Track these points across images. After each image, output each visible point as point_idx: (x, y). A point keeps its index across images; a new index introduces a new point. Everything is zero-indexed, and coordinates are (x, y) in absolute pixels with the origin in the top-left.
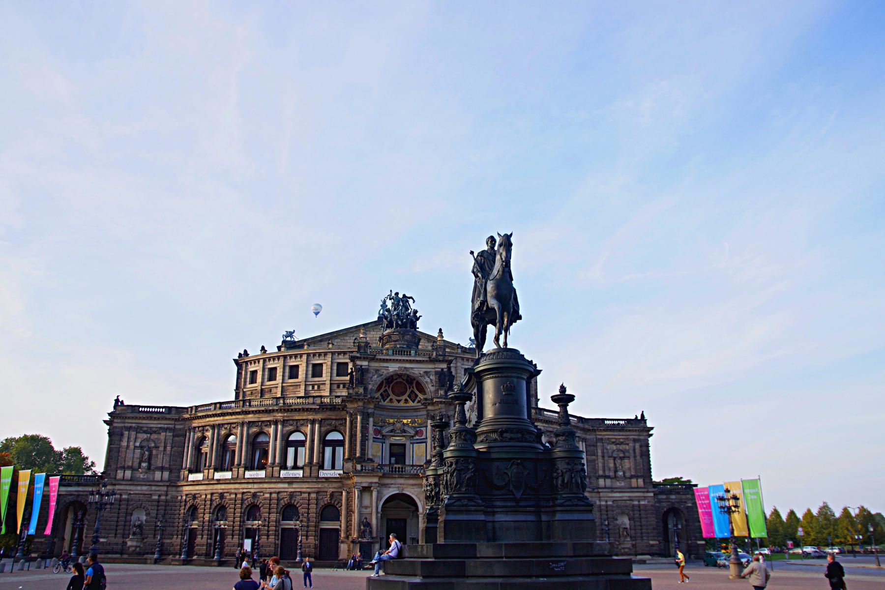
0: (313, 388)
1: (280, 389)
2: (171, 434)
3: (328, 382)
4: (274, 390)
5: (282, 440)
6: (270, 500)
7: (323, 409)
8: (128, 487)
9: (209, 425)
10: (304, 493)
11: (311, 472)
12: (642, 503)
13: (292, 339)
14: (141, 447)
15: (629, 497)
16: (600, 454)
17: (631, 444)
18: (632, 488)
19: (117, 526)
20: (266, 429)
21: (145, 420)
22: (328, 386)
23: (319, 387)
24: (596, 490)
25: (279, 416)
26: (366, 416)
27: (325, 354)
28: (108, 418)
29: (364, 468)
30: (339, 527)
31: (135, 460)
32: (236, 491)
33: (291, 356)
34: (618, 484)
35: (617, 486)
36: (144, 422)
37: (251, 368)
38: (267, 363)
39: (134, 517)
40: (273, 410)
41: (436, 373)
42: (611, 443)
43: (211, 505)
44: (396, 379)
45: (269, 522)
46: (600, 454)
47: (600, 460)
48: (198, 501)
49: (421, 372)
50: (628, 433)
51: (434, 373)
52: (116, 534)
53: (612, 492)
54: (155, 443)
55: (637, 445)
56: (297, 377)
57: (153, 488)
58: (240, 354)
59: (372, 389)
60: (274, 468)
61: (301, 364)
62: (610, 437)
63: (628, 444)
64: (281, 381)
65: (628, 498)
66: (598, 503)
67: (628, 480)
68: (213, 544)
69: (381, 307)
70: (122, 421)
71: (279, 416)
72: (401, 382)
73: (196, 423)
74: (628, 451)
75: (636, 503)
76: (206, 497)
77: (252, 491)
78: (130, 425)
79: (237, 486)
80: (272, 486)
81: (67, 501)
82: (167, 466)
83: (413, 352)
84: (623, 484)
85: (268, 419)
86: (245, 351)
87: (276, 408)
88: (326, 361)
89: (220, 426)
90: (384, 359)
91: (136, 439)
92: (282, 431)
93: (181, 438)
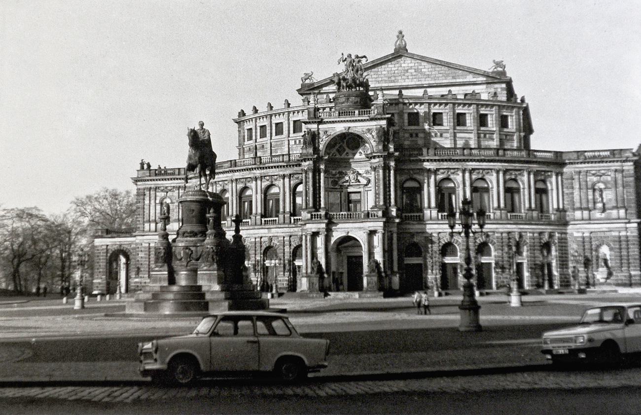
0: (295, 142)
7: (290, 166)
10: (280, 236)
11: (284, 219)
12: (623, 233)
18: (613, 219)
20: (248, 185)
25: (258, 173)
29: (313, 217)
35: (596, 218)
37: (247, 126)
38: (258, 121)
42: (591, 175)
46: (577, 186)
49: (364, 130)
54: (171, 200)
55: (619, 176)
65: (607, 230)
69: (397, 39)
70: (144, 183)
75: (616, 234)
78: (149, 186)
81: (113, 250)
86: (242, 111)
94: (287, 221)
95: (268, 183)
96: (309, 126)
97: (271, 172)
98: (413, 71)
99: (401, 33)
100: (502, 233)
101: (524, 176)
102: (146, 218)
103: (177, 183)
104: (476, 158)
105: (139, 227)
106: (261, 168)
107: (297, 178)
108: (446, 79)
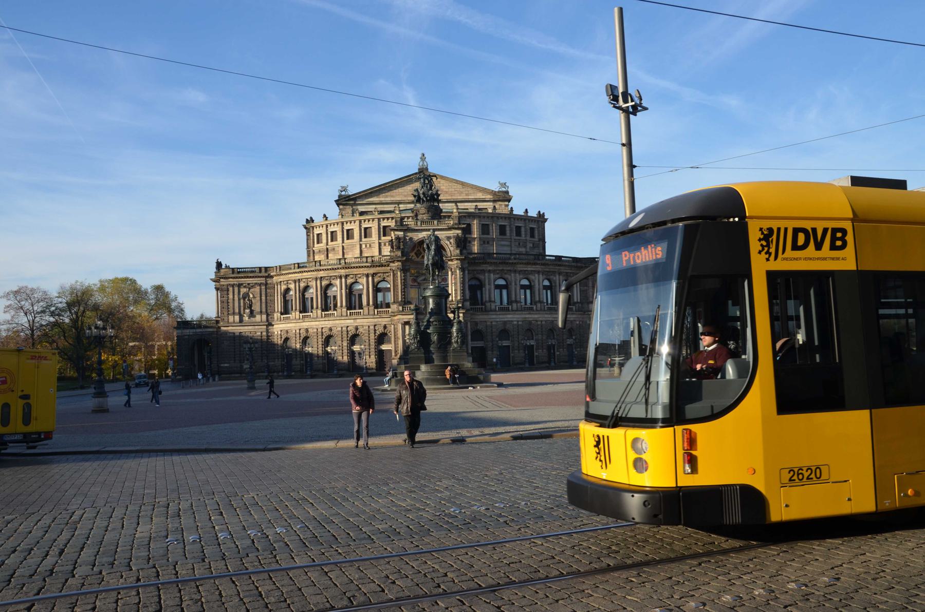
0: (366, 246)
1: (341, 248)
3: (377, 242)
4: (336, 249)
5: (346, 289)
10: (365, 326)
13: (347, 193)
19: (235, 355)
20: (333, 282)
21: (244, 278)
23: (370, 246)
24: (586, 313)
25: (343, 272)
27: (373, 220)
28: (213, 277)
30: (391, 348)
36: (242, 280)
37: (317, 231)
40: (338, 268)
41: (454, 237)
45: (342, 347)
46: (590, 285)
52: (235, 360)
57: (256, 327)
58: (307, 220)
59: (407, 252)
60: (343, 310)
64: (341, 242)
68: (304, 364)
71: (343, 272)
77: (329, 326)
79: (317, 323)
80: (343, 322)
83: (436, 222)
86: (311, 218)
87: (340, 266)
88: (374, 225)
91: (239, 292)
94: (371, 312)
95: (352, 280)
96: (397, 233)
97: (355, 271)
99: (423, 155)
100: (542, 321)
101: (555, 276)
102: (231, 311)
104: (524, 262)
107: (380, 277)
108: (460, 196)
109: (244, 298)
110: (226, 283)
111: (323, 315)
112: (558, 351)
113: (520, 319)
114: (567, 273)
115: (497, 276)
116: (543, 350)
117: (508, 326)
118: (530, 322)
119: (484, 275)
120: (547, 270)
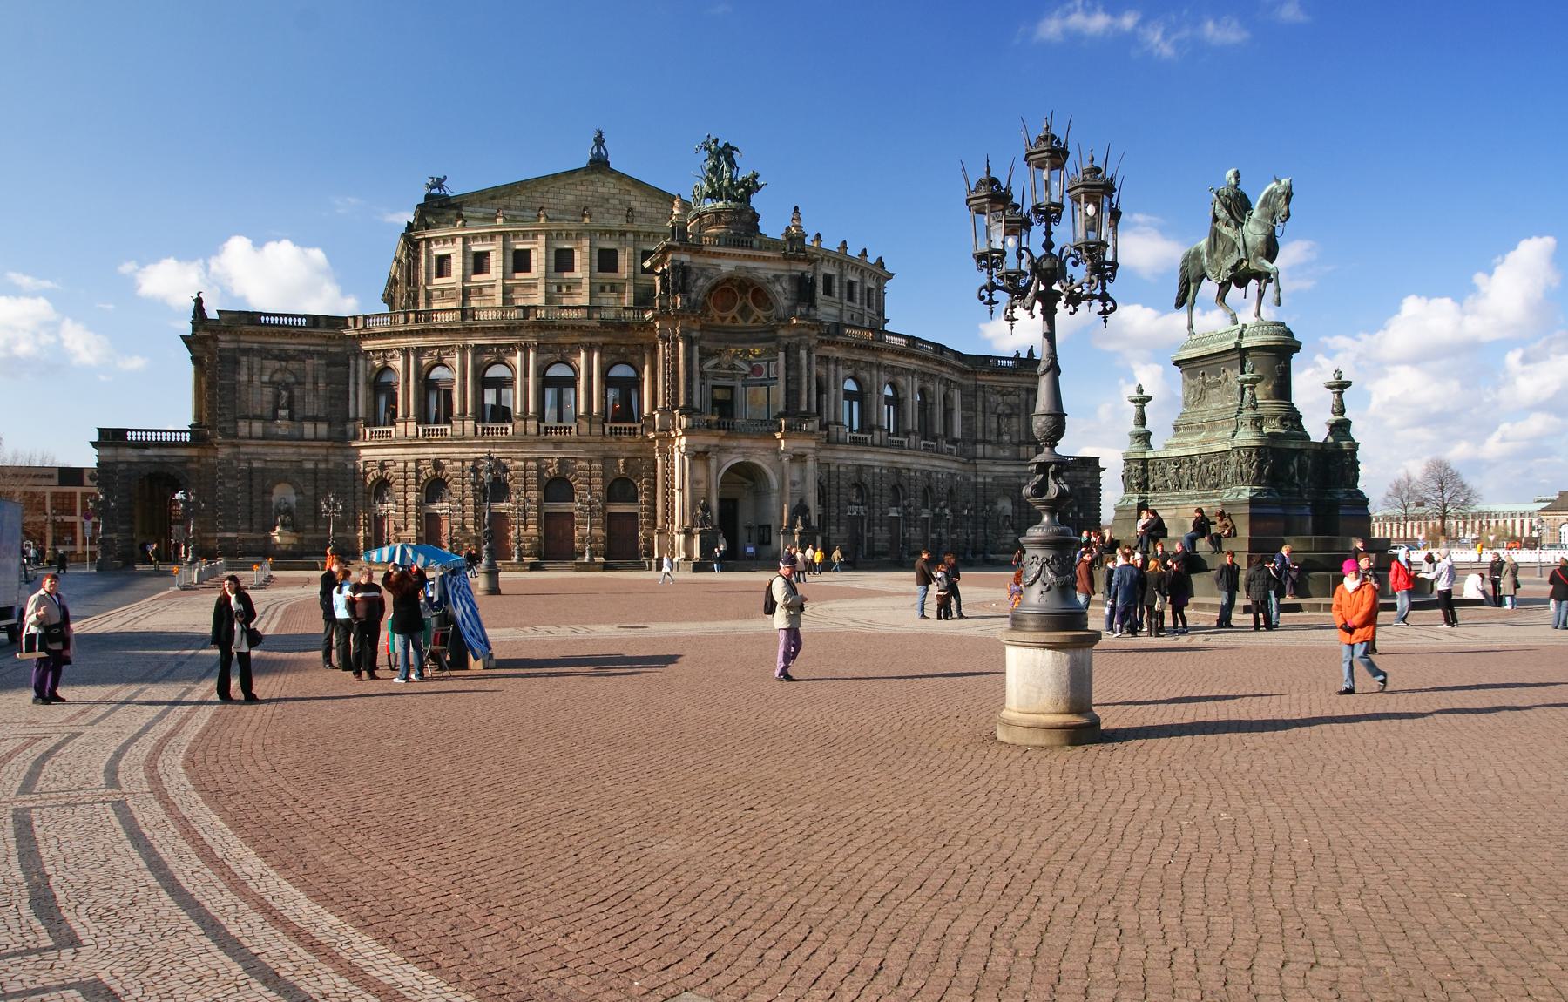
0: (559, 289)
1: (498, 290)
2: (323, 362)
3: (586, 281)
6: (525, 471)
8: (260, 450)
9: (398, 349)
10: (581, 459)
13: (443, 192)
14: (272, 383)
15: (1015, 472)
16: (980, 408)
17: (1023, 396)
22: (585, 289)
23: (569, 288)
24: (971, 462)
26: (690, 344)
28: (189, 332)
31: (265, 406)
32: (463, 456)
33: (516, 235)
34: (1001, 453)
39: (275, 498)
41: (792, 278)
43: (417, 478)
44: (723, 284)
46: (980, 408)
47: (980, 418)
48: (391, 471)
49: (769, 276)
50: (1020, 379)
51: (787, 278)
53: (994, 464)
54: (296, 377)
56: (528, 269)
57: (304, 451)
61: (536, 249)
62: (996, 384)
63: (1019, 396)
66: (973, 480)
67: (1015, 448)
70: (234, 338)
72: (728, 290)
73: (368, 345)
74: (1018, 406)
76: (406, 466)
78: (248, 345)
82: (322, 415)
84: (1007, 454)
85: (511, 341)
89: (419, 351)
90: (715, 253)
92: (536, 362)
93: (341, 369)
98: (617, 202)
103: (312, 345)
105: (225, 428)
106: (540, 327)
109: (272, 383)
110: (232, 345)
111: (480, 431)
112: (933, 532)
113: (884, 464)
114: (947, 379)
115: (849, 372)
116: (838, 526)
117: (867, 478)
118: (898, 472)
119: (827, 369)
120: (925, 370)
